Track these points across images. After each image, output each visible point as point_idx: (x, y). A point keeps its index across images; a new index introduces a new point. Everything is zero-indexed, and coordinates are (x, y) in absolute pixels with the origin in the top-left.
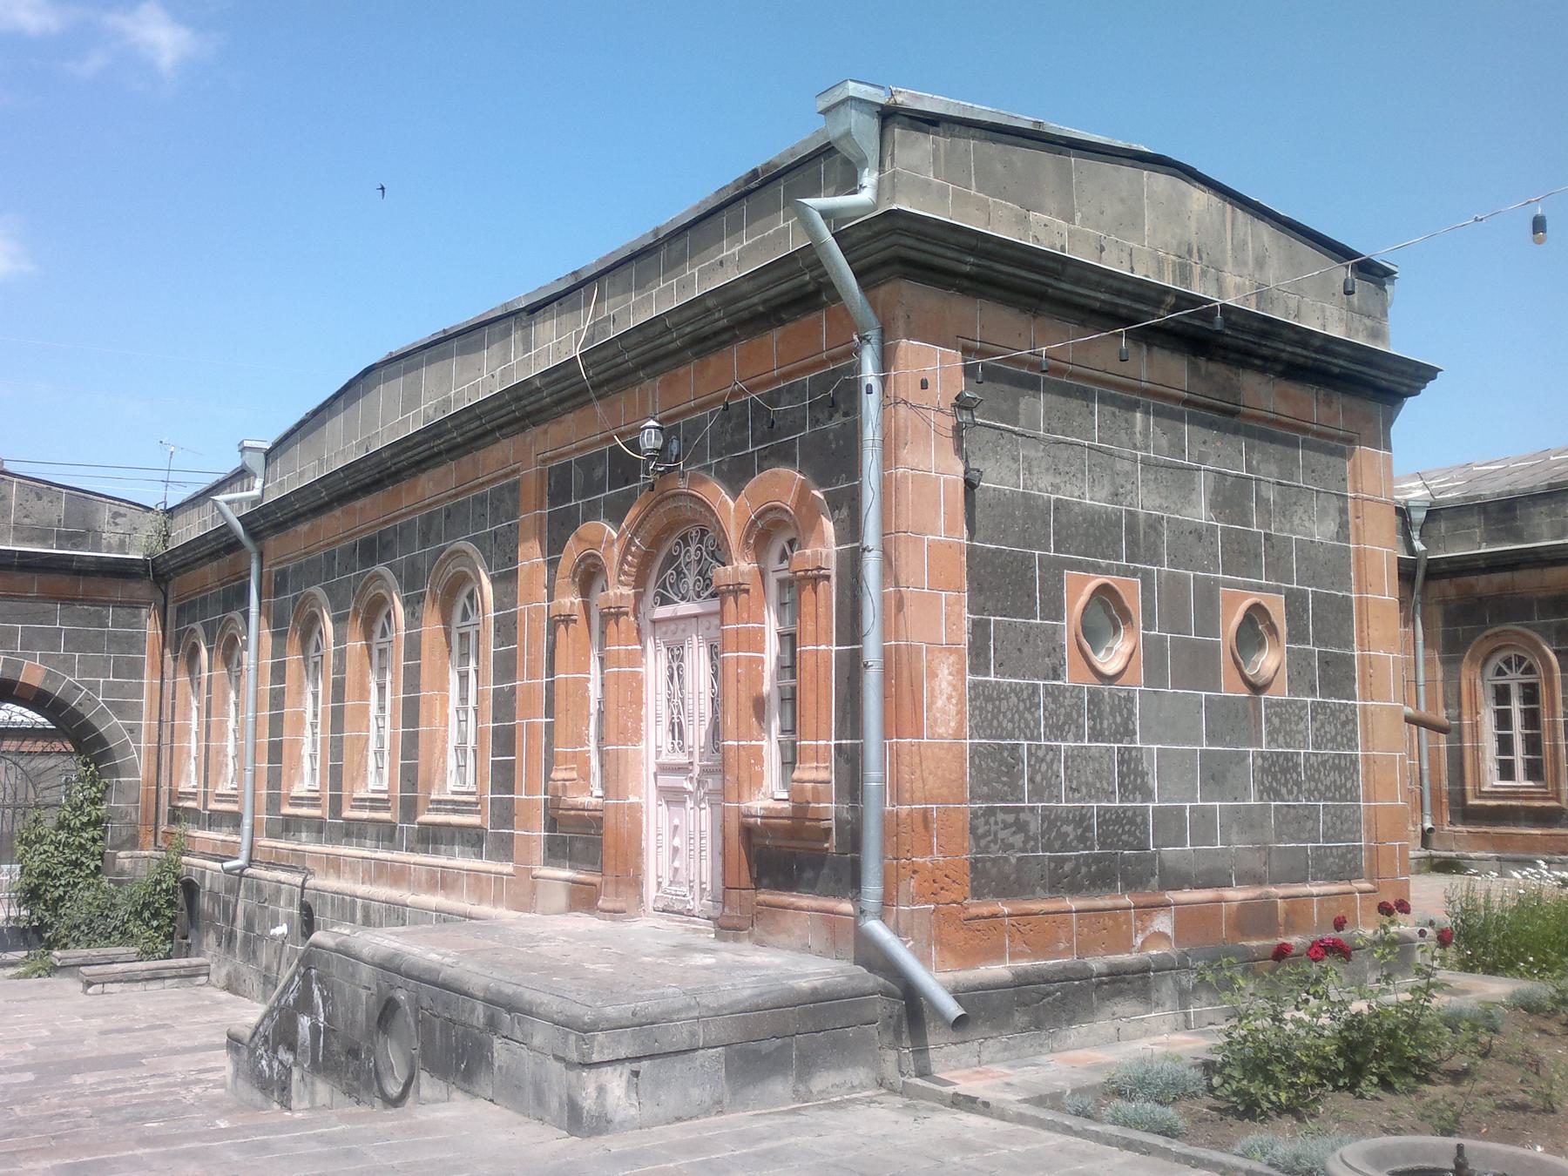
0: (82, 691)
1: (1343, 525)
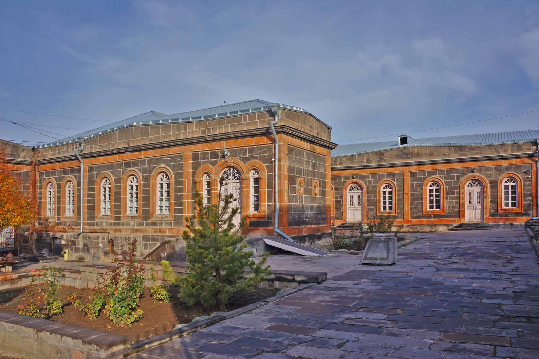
1: (325, 169)
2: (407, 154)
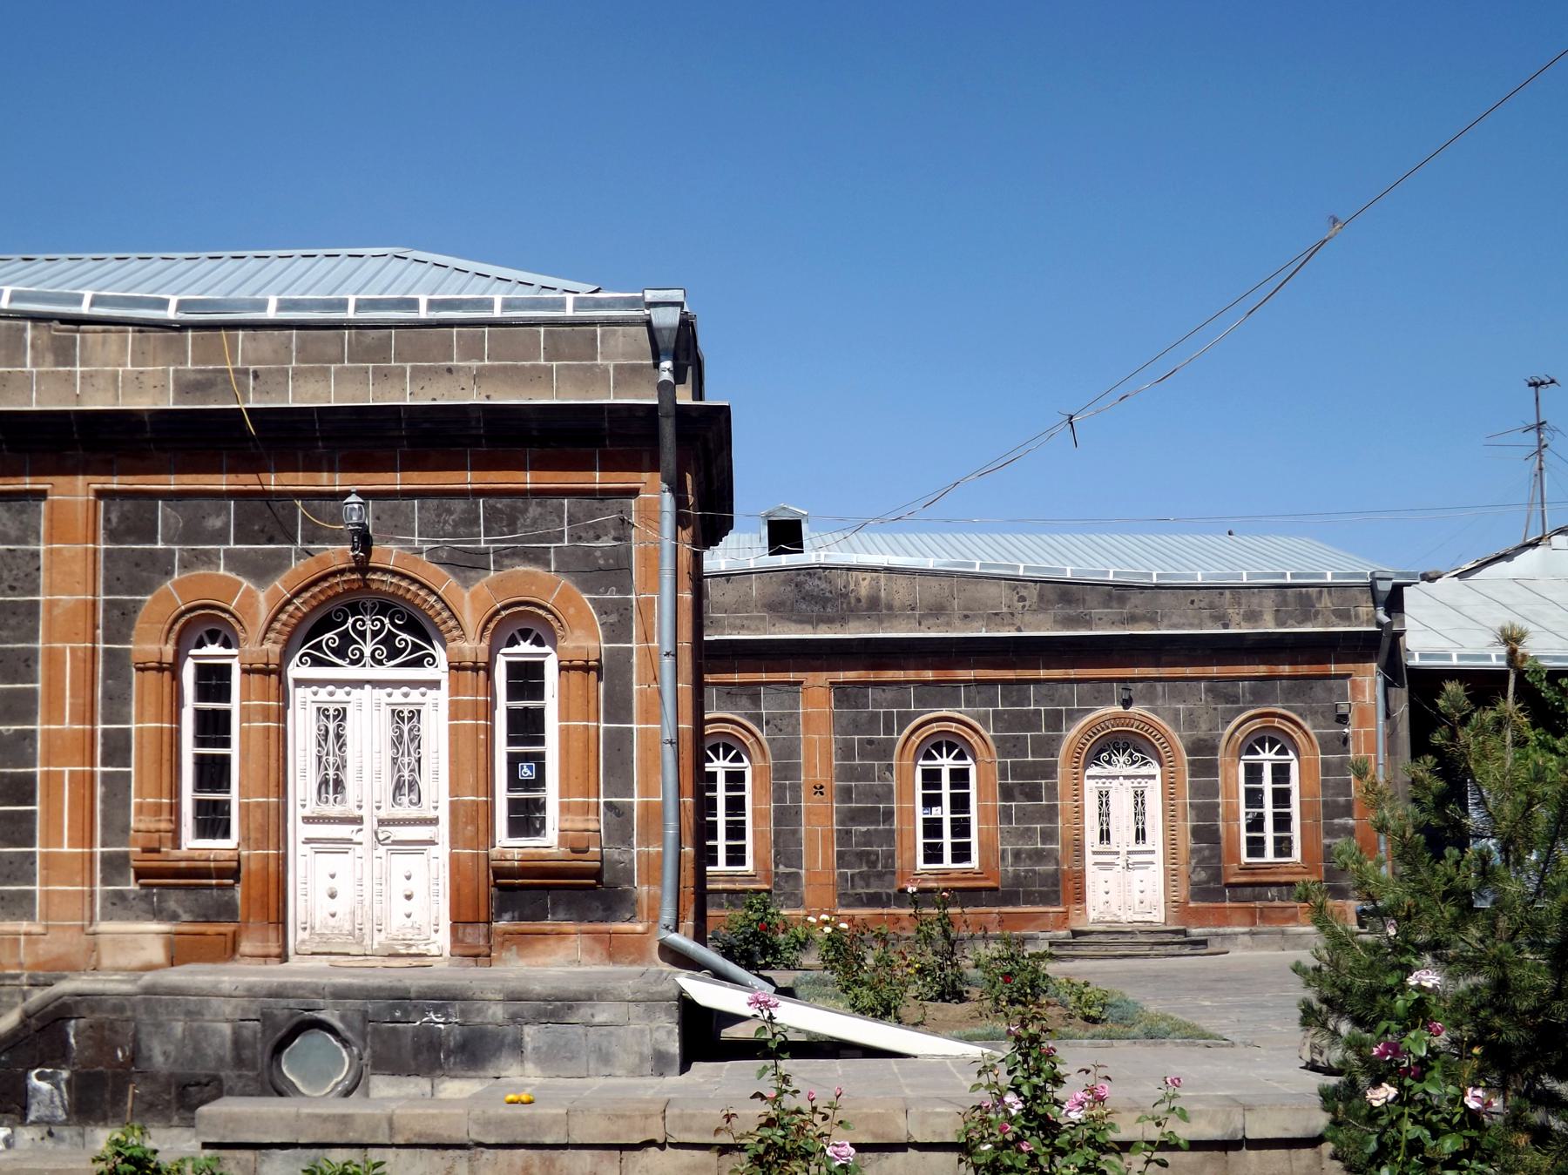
2: (821, 600)
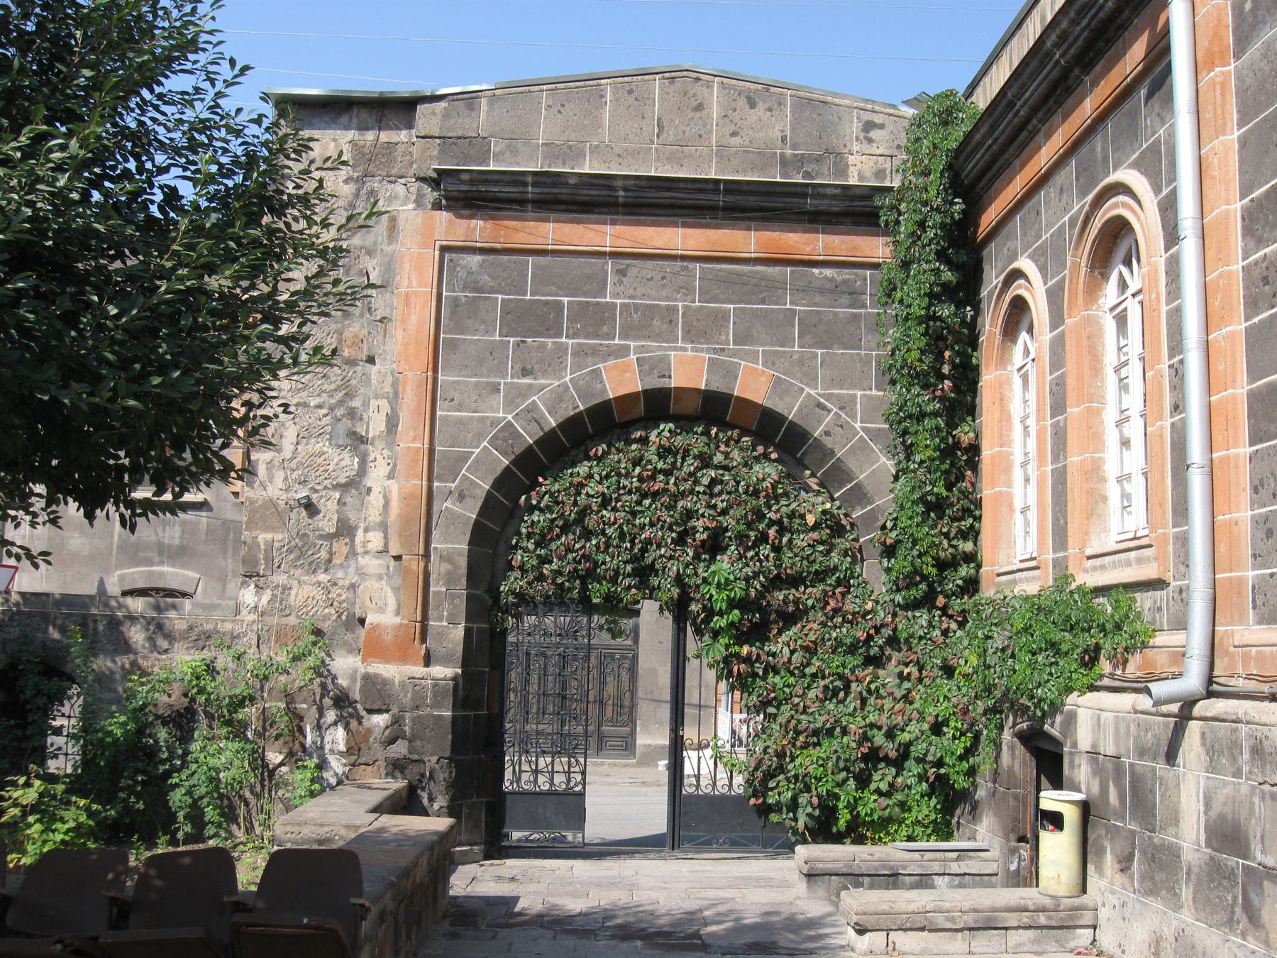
0: (829, 411)
